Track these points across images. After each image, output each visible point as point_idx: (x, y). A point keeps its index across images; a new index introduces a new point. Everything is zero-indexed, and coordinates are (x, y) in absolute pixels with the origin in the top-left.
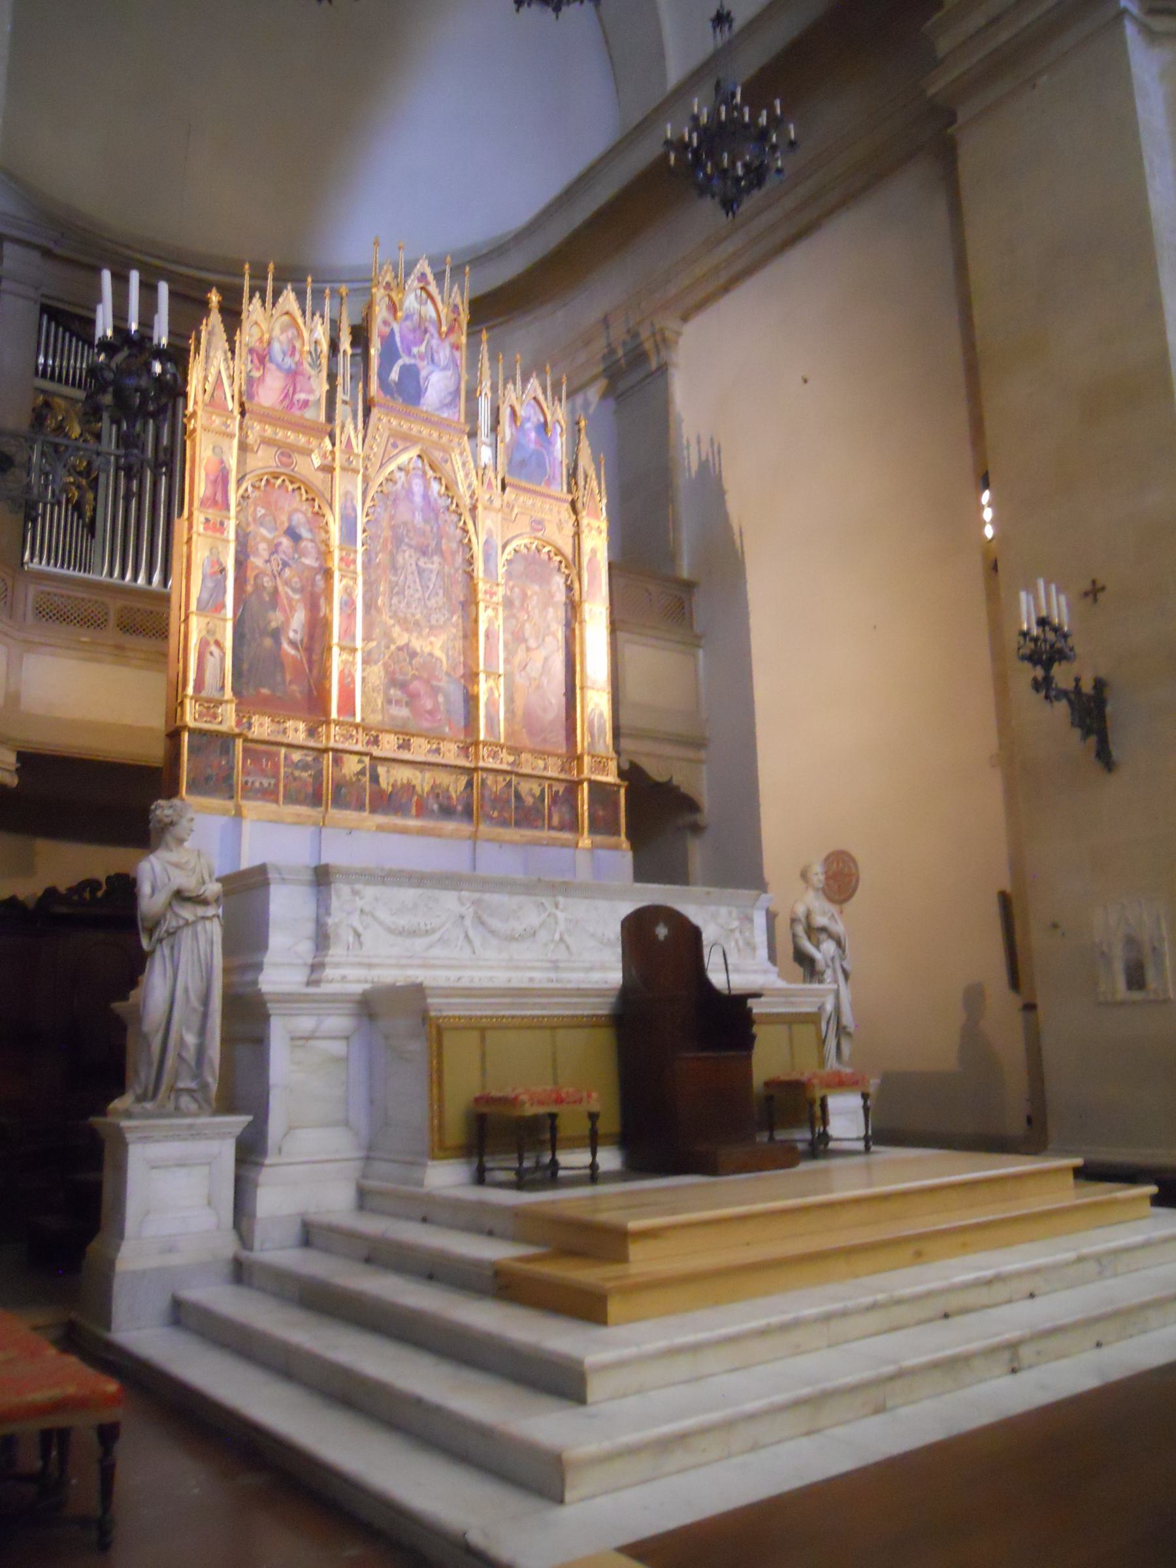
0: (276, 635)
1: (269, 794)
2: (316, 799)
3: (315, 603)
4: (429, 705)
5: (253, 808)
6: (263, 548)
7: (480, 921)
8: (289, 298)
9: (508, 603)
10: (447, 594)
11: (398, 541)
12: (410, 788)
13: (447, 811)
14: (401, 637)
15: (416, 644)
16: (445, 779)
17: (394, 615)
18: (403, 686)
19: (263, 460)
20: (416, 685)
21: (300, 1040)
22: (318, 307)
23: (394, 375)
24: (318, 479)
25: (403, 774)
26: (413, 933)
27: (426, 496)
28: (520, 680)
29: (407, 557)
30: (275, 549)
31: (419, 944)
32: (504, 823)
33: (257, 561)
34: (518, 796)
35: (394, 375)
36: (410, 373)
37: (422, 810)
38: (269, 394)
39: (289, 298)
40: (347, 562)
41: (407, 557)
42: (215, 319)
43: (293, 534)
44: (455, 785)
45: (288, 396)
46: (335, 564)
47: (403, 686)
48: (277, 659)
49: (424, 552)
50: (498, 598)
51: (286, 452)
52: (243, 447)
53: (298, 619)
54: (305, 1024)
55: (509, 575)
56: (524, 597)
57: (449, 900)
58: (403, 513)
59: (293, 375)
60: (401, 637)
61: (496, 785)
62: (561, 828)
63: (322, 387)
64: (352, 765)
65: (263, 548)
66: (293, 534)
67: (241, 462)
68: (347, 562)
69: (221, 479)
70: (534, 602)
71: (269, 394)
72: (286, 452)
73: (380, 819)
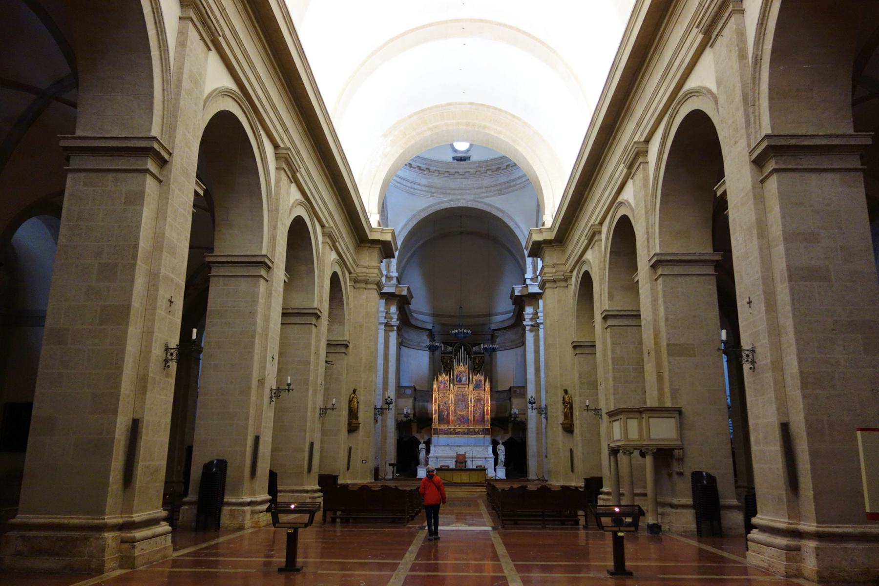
0: (443, 415)
1: (442, 434)
2: (447, 434)
3: (448, 410)
4: (463, 421)
5: (440, 436)
6: (442, 406)
7: (451, 449)
8: (444, 375)
9: (474, 406)
10: (466, 406)
11: (459, 401)
12: (460, 432)
13: (465, 434)
14: (459, 413)
15: (461, 413)
16: (465, 430)
17: (458, 410)
18: (459, 419)
19: (441, 395)
20: (461, 419)
21: (431, 461)
22: (447, 374)
23: (458, 379)
24: (448, 396)
25: (459, 430)
26: (443, 451)
27: (462, 394)
28: (476, 416)
29: (460, 403)
30: (443, 405)
31: (444, 452)
32: (472, 435)
33: (441, 407)
34: (475, 431)
35: (458, 379)
36: (460, 379)
37: (462, 434)
38: (442, 387)
39: (444, 375)
40: (452, 405)
41: (460, 403)
42: (435, 380)
43: (445, 403)
44: (466, 431)
45: (444, 387)
46: (450, 405)
47: (459, 419)
48: (443, 418)
49: (462, 401)
50: (472, 405)
51: (444, 393)
52: (438, 394)
53: (446, 413)
54: (432, 459)
55: (474, 402)
56: (477, 404)
57: (447, 448)
58: (459, 397)
59: (445, 384)
60: (459, 413)
61: (471, 430)
62: (482, 434)
63: (448, 385)
64: (452, 430)
65: (442, 406)
66: (445, 403)
67: (438, 396)
68: (452, 405)
69: (436, 399)
70: (478, 405)
71: (442, 387)
72: (444, 393)
73: (456, 436)
